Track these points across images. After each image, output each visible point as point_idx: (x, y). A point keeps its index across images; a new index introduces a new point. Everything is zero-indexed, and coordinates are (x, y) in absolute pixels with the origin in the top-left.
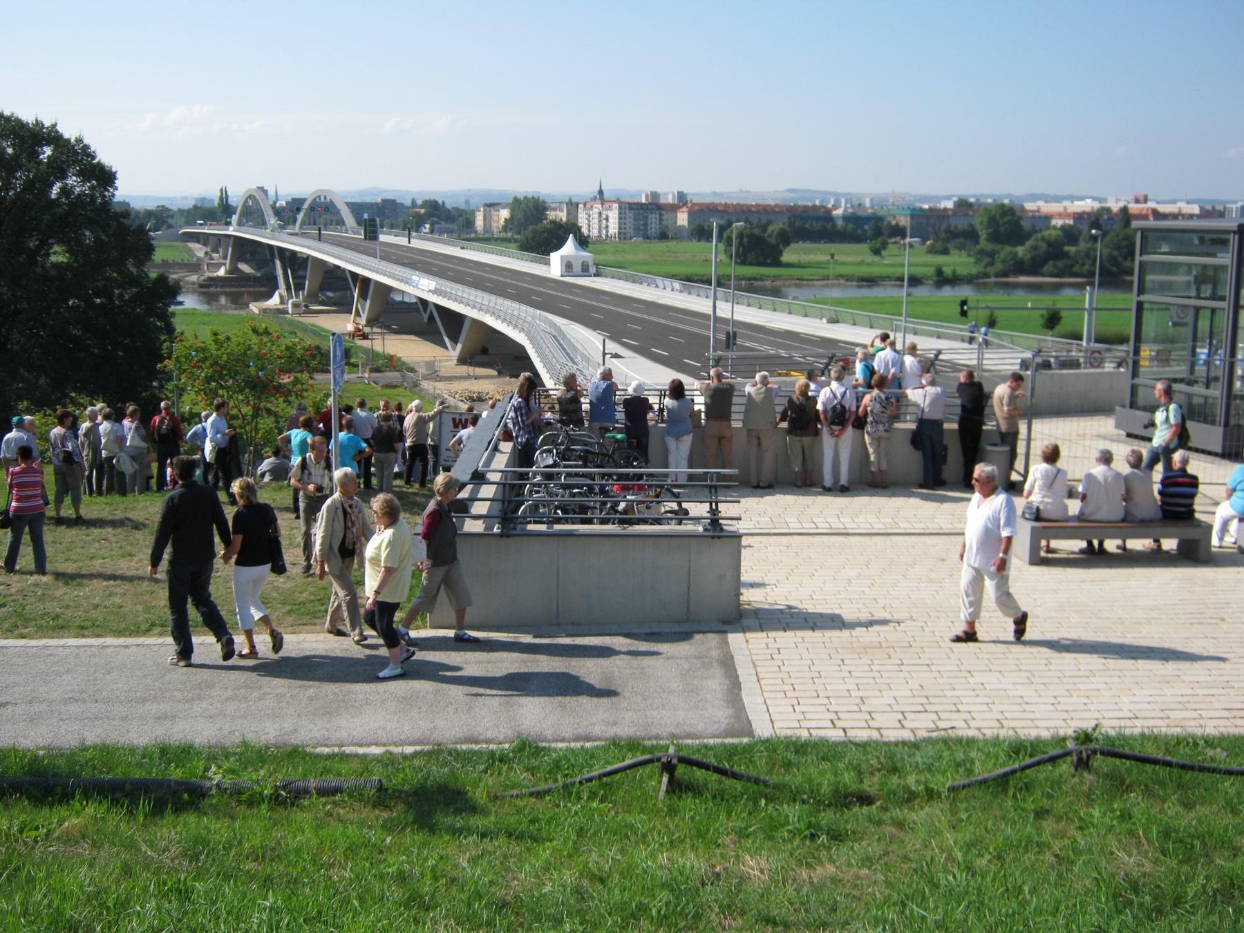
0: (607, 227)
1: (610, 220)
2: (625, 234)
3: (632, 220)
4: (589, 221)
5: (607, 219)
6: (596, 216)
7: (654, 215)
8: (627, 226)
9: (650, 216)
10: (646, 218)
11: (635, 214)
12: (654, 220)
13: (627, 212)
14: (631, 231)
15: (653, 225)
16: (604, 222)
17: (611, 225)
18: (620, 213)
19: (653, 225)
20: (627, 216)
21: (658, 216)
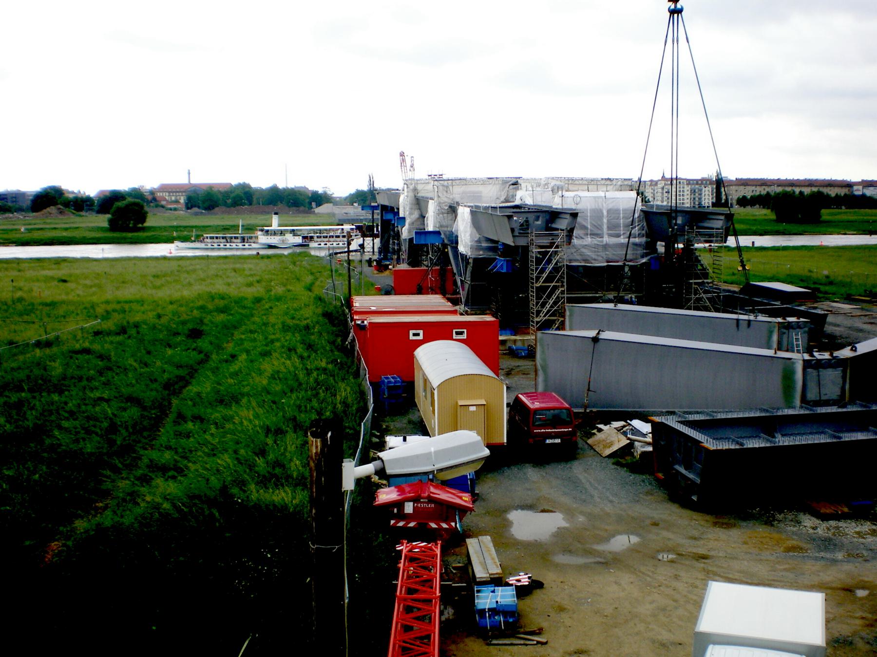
3: (689, 193)
4: (654, 194)
6: (660, 190)
7: (707, 189)
8: (685, 198)
9: (704, 189)
10: (701, 190)
12: (707, 193)
13: (686, 186)
14: (689, 201)
15: (707, 197)
16: (666, 194)
19: (707, 197)
20: (685, 191)
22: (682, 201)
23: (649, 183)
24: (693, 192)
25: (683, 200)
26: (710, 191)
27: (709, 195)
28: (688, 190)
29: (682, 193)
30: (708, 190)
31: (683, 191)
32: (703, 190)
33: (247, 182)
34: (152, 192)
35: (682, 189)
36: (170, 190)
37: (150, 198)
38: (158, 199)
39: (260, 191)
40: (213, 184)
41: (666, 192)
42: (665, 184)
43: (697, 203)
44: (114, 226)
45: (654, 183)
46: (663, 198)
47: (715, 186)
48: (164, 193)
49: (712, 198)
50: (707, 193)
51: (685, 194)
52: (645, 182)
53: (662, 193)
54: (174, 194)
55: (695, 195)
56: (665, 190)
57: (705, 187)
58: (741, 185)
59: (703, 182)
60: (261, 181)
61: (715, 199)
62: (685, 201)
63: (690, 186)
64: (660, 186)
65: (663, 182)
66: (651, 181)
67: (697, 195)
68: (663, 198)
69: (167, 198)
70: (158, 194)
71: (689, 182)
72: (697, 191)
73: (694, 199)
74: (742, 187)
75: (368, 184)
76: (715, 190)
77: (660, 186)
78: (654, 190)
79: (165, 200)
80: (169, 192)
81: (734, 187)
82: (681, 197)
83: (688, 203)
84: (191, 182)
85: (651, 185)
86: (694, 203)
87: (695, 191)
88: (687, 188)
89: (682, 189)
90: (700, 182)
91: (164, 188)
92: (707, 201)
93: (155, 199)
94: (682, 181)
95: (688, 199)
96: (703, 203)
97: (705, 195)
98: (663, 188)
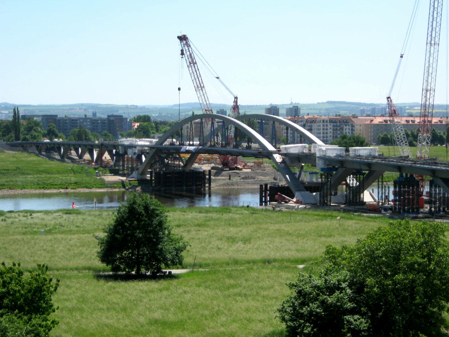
3: (331, 130)
7: (347, 127)
9: (345, 127)
11: (333, 126)
13: (328, 124)
14: (331, 138)
20: (328, 128)
21: (350, 127)
22: (325, 139)
26: (350, 129)
28: (331, 128)
31: (327, 129)
32: (344, 129)
50: (347, 131)
57: (346, 126)
62: (328, 139)
63: (332, 124)
71: (331, 121)
87: (337, 130)
88: (330, 126)
95: (330, 136)
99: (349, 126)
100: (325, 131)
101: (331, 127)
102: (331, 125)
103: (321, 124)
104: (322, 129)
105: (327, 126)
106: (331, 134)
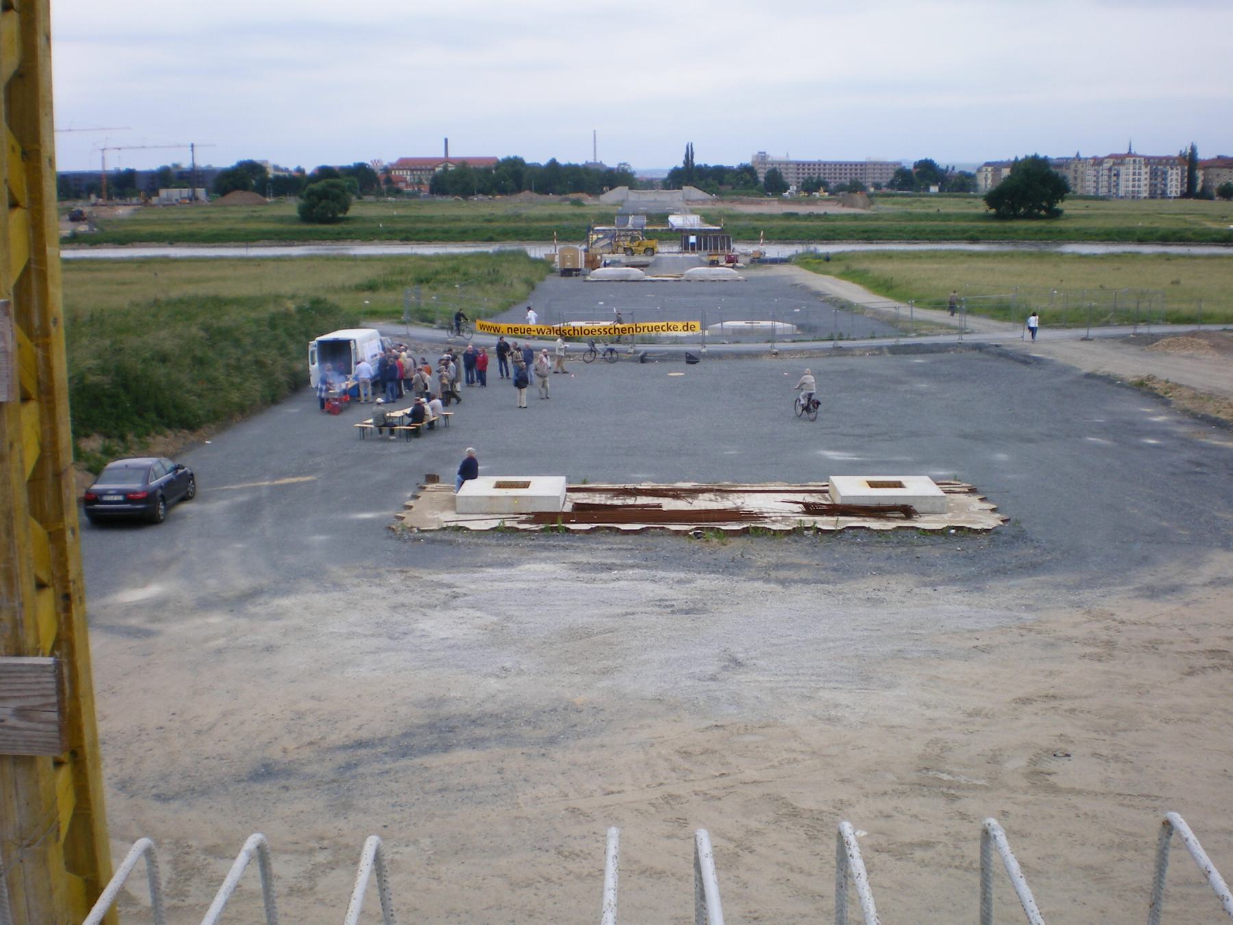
0: (1117, 185)
1: (1122, 177)
2: (1139, 192)
3: (1148, 176)
4: (1098, 178)
5: (1117, 175)
6: (1106, 172)
7: (1174, 171)
8: (1142, 183)
10: (1165, 173)
12: (1174, 177)
13: (1143, 167)
14: (1147, 188)
15: (1174, 183)
16: (1114, 179)
17: (1122, 183)
18: (1134, 169)
19: (1174, 183)
21: (1179, 172)
22: (1136, 189)
23: (1092, 161)
24: (1153, 174)
25: (1139, 186)
26: (1180, 174)
27: (1176, 179)
29: (1137, 177)
30: (1177, 173)
31: (1139, 174)
33: (520, 155)
34: (387, 170)
35: (1137, 171)
36: (413, 167)
37: (382, 178)
38: (394, 179)
39: (535, 168)
40: (469, 159)
41: (1115, 175)
42: (1114, 164)
43: (1159, 192)
44: (307, 216)
45: (1098, 162)
46: (1110, 184)
47: (1186, 168)
48: (401, 173)
49: (1182, 186)
51: (1143, 177)
52: (1086, 159)
53: (1110, 177)
54: (419, 173)
55: (1156, 179)
56: (1114, 172)
57: (1172, 169)
58: (1224, 167)
59: (1168, 161)
60: (536, 156)
61: (1186, 186)
64: (1107, 166)
65: (1111, 161)
66: (1095, 158)
67: (1159, 179)
68: (1110, 184)
69: (408, 178)
70: (393, 173)
71: (1149, 161)
72: (1159, 173)
73: (1156, 185)
74: (1225, 170)
75: (683, 158)
76: (1186, 174)
77: (1107, 166)
78: (1098, 172)
79: (404, 180)
80: (412, 170)
81: (1214, 169)
82: (1137, 183)
83: (1145, 191)
84: (450, 156)
85: (1093, 165)
86: (1155, 191)
87: (1156, 173)
89: (1137, 171)
90: (1164, 161)
91: (404, 164)
92: (1174, 189)
93: (389, 181)
94: (1138, 159)
95: (1146, 185)
96: (1168, 192)
97: (1171, 180)
98: (1110, 169)
99: (1177, 169)
100: (1137, 177)
101: (1148, 170)
102: (1146, 167)
103: (1131, 167)
104: (1131, 173)
105: (1140, 169)
106: (1147, 182)
